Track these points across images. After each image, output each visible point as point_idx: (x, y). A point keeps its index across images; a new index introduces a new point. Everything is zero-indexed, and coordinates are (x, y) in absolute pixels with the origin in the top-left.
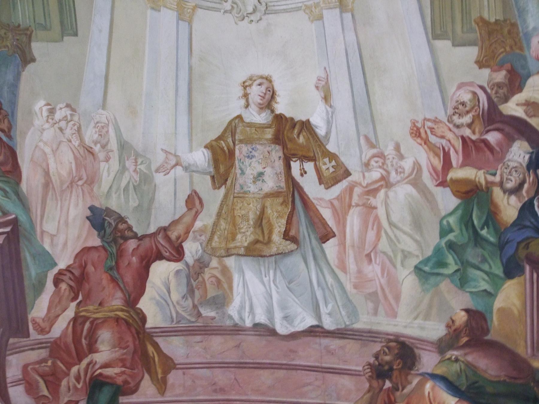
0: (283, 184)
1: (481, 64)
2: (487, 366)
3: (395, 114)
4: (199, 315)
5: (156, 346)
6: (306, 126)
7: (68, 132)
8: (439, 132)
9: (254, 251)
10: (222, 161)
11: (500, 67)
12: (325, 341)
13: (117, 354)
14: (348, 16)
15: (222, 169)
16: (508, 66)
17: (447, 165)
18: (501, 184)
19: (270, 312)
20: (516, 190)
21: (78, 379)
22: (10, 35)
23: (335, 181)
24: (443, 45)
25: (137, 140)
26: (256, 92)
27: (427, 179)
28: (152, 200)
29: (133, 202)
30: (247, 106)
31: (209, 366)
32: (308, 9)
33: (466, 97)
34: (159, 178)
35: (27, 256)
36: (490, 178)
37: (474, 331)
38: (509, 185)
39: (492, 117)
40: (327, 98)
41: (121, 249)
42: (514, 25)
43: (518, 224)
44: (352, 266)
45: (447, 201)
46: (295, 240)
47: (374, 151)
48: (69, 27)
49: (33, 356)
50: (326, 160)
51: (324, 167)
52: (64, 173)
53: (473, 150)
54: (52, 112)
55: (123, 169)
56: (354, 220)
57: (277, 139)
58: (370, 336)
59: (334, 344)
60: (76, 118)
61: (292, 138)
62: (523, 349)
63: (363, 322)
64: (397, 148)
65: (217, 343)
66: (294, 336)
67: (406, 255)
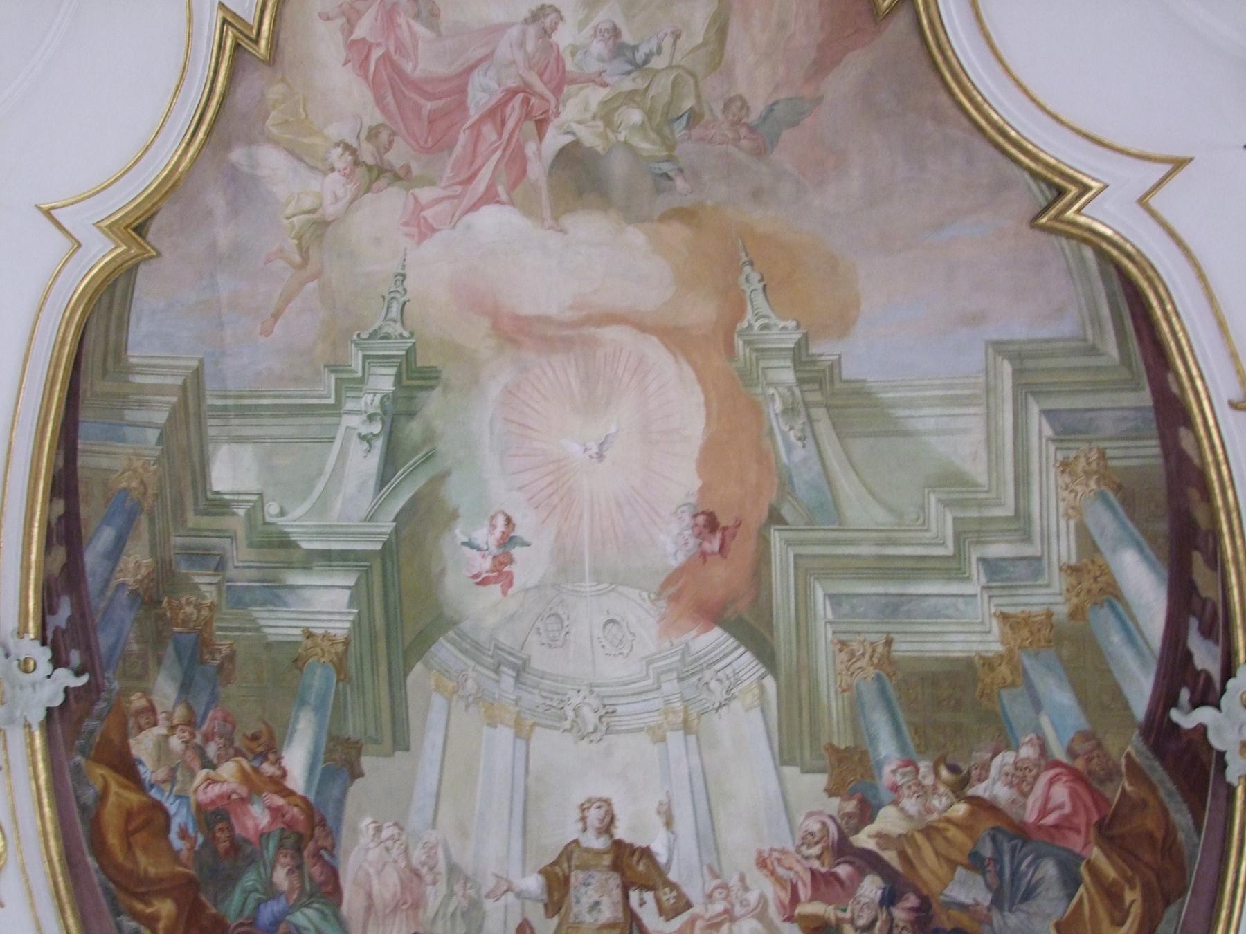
0: (620, 915)
1: (831, 792)
3: (740, 844)
6: (646, 853)
7: (395, 852)
8: (787, 862)
10: (557, 886)
11: (850, 797)
14: (692, 739)
15: (556, 896)
16: (858, 795)
17: (795, 899)
18: (852, 921)
22: (339, 748)
23: (676, 912)
24: (791, 772)
25: (467, 862)
26: (594, 815)
27: (773, 913)
28: (481, 927)
30: (585, 830)
32: (651, 730)
33: (815, 826)
34: (489, 905)
36: (841, 914)
38: (861, 922)
39: (842, 849)
40: (669, 824)
42: (864, 753)
47: (717, 882)
48: (400, 739)
50: (667, 890)
51: (664, 898)
52: (388, 896)
53: (823, 883)
54: (378, 830)
55: (451, 894)
57: (616, 866)
60: (404, 837)
61: (631, 865)
64: (742, 879)
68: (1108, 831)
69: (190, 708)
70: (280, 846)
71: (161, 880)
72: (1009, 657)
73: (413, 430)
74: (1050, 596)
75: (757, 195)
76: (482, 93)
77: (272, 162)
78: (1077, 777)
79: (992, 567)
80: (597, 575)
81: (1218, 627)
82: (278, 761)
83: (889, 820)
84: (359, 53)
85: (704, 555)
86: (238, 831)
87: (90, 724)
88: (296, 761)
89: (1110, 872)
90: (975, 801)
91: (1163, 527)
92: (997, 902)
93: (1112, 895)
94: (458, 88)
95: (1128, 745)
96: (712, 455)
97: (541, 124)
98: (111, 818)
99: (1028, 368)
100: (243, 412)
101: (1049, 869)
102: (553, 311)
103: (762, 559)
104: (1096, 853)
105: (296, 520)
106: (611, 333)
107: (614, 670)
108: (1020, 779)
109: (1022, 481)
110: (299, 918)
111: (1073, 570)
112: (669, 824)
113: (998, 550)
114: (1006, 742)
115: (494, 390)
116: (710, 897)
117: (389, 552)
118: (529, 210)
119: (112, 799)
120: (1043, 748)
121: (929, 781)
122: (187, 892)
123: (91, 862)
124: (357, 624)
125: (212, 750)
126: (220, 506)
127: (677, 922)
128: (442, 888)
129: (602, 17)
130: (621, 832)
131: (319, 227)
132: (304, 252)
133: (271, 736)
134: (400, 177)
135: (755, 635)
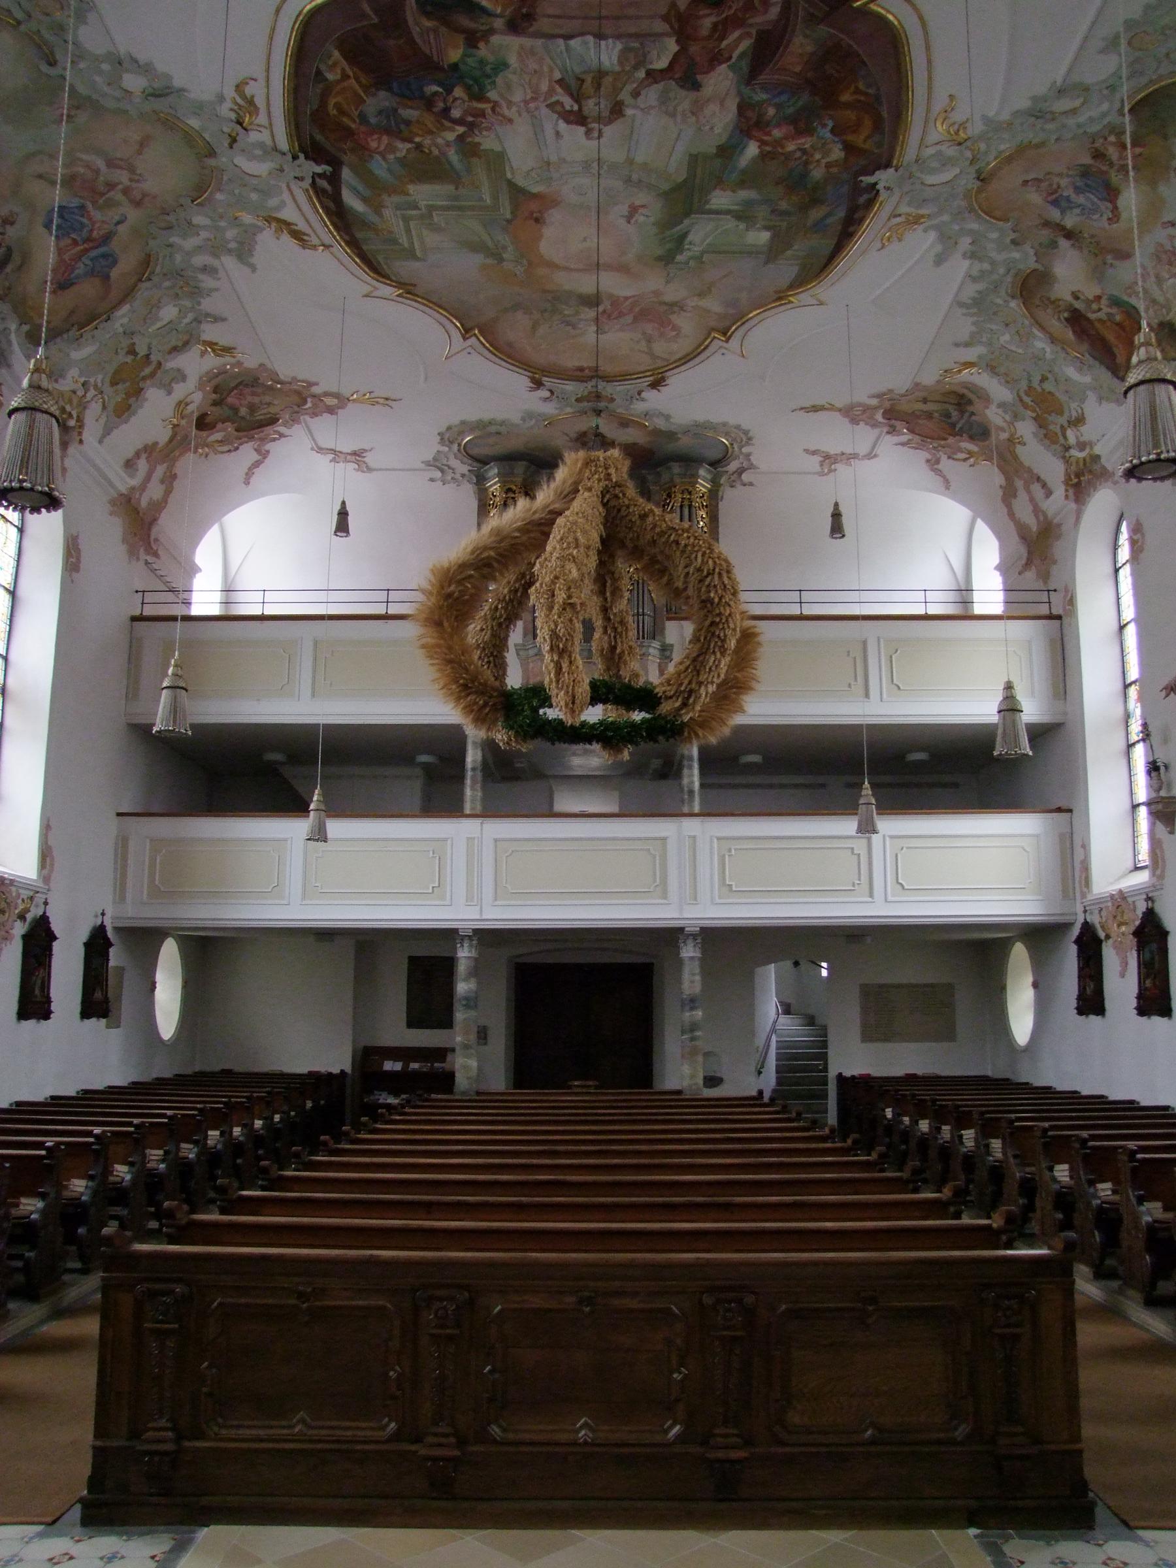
2: (465, 22)
3: (522, 126)
4: (642, 44)
5: (672, 27)
6: (568, 122)
10: (617, 111)
11: (469, 143)
12: (562, 32)
20: (455, 99)
21: (730, 7)
24: (498, 148)
27: (504, 104)
29: (672, 95)
31: (638, 17)
33: (485, 133)
34: (655, 103)
35: (746, 70)
37: (472, 40)
40: (557, 133)
41: (686, 74)
43: (454, 87)
44: (546, 69)
45: (492, 95)
46: (578, 79)
48: (694, 160)
49: (758, 19)
54: (712, 128)
56: (544, 87)
59: (557, 31)
61: (578, 118)
63: (539, 42)
65: (633, 30)
66: (582, 34)
67: (515, 73)
68: (349, 133)
73: (668, 246)
74: (390, 201)
76: (629, 319)
79: (416, 208)
81: (319, 192)
83: (451, 136)
85: (540, 212)
86: (791, 128)
89: (345, 119)
90: (410, 141)
92: (396, 110)
93: (342, 112)
94: (636, 319)
97: (604, 311)
98: (865, 131)
100: (750, 253)
101: (373, 120)
104: (353, 126)
105: (730, 223)
109: (408, 231)
110: (765, 96)
111: (383, 207)
112: (557, 133)
113: (414, 212)
114: (402, 161)
116: (537, 109)
117: (687, 214)
118: (611, 296)
119: (862, 137)
120: (384, 158)
121: (433, 149)
123: (885, 114)
125: (798, 154)
126: (767, 228)
127: (554, 99)
128: (680, 109)
130: (582, 129)
131: (701, 295)
132: (709, 289)
135: (518, 194)
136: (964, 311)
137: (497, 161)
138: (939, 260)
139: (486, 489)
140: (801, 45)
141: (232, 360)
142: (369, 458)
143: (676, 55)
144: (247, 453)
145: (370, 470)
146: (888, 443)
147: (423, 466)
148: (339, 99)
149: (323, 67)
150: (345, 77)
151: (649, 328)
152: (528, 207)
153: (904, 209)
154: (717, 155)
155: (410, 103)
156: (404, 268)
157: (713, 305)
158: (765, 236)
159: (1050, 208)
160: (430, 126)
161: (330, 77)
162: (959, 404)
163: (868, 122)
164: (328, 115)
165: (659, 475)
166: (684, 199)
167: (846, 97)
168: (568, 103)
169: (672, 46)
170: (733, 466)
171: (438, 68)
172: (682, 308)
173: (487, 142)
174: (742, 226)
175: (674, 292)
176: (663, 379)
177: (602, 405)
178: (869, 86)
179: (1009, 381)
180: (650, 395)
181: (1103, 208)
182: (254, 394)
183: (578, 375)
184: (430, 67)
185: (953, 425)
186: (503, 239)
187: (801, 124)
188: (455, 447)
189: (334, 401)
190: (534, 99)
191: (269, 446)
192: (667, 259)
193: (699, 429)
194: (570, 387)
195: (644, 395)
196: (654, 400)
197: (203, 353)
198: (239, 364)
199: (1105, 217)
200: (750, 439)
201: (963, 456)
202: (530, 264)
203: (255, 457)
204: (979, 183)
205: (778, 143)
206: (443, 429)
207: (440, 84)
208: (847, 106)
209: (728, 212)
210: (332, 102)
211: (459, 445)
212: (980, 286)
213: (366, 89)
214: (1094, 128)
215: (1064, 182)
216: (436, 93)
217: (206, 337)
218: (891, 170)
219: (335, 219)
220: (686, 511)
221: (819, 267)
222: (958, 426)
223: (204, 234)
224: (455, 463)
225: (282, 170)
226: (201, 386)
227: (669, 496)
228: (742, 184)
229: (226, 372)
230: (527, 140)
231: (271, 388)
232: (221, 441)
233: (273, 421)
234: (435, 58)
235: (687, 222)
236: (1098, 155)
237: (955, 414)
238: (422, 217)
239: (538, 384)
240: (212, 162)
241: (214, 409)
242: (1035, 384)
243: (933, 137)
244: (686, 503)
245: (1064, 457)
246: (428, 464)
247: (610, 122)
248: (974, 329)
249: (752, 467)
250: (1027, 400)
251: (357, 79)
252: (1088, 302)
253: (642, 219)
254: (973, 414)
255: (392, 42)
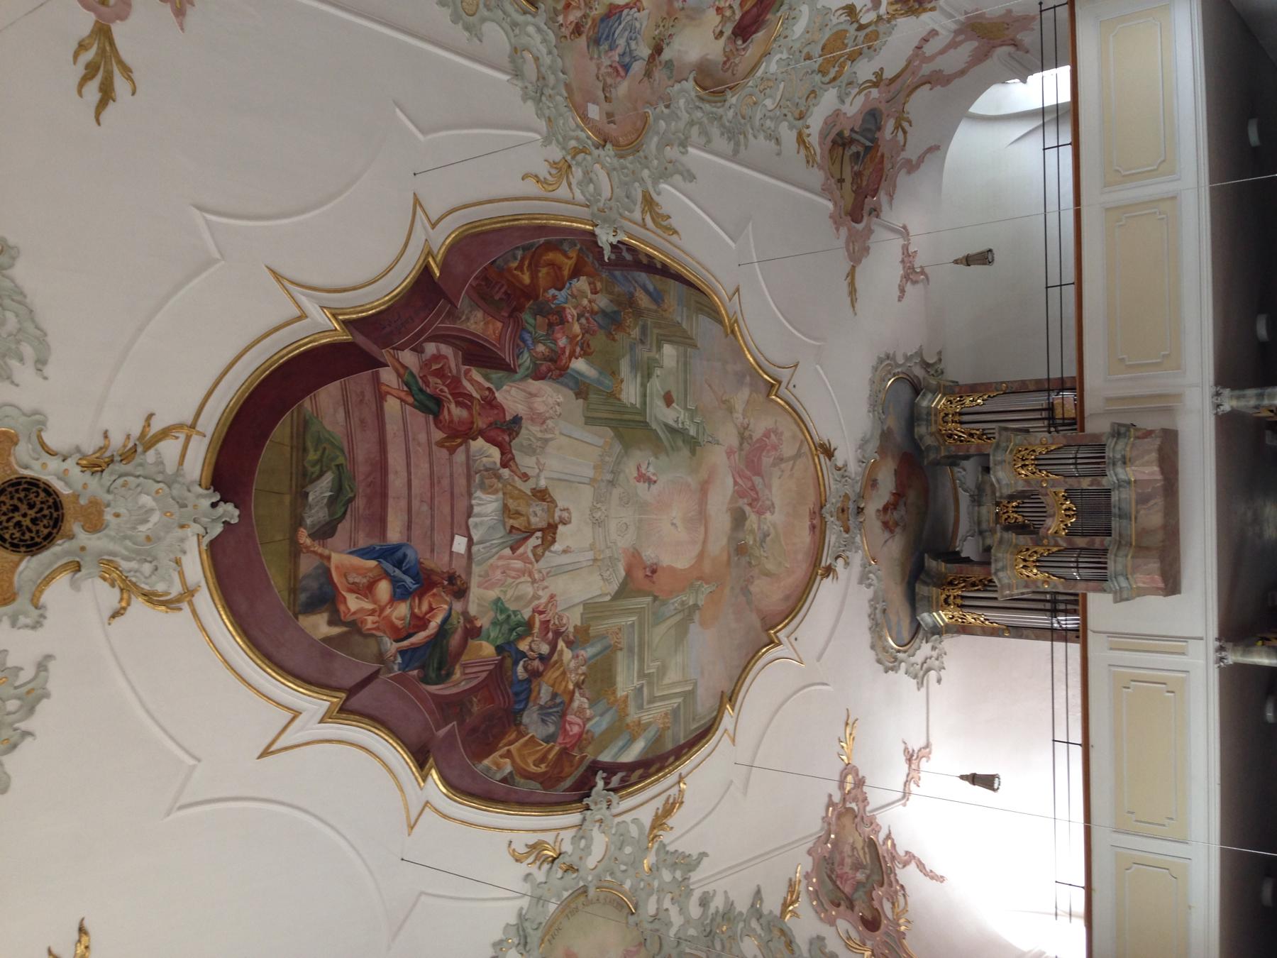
1: (575, 627)
3: (558, 585)
5: (460, 445)
6: (554, 541)
9: (505, 508)
10: (542, 495)
13: (456, 419)
19: (479, 515)
20: (531, 649)
21: (442, 391)
23: (534, 555)
24: (580, 609)
26: (565, 515)
27: (536, 602)
29: (525, 443)
31: (452, 475)
34: (534, 459)
35: (501, 374)
37: (473, 632)
40: (565, 552)
41: (504, 431)
44: (500, 563)
45: (527, 614)
46: (511, 532)
48: (590, 421)
49: (453, 365)
54: (558, 404)
56: (518, 564)
58: (469, 573)
61: (550, 532)
62: (465, 658)
63: (476, 569)
67: (505, 592)
68: (565, 753)
69: (596, 313)
70: (552, 350)
71: (537, 277)
72: (616, 701)
73: (680, 443)
74: (633, 715)
75: (732, 588)
76: (757, 480)
77: (745, 393)
78: (580, 735)
79: (640, 689)
80: (641, 521)
81: (624, 785)
82: (580, 356)
83: (568, 654)
84: (767, 434)
87: (591, 256)
88: (579, 365)
89: (551, 756)
90: (573, 692)
91: (650, 756)
92: (542, 708)
93: (543, 759)
94: (758, 474)
95: (590, 754)
96: (672, 570)
97: (750, 505)
99: (689, 696)
100: (685, 364)
101: (552, 729)
102: (709, 507)
103: (646, 594)
104: (557, 748)
106: (702, 529)
107: (613, 525)
108: (581, 710)
109: (663, 698)
112: (565, 552)
113: (645, 690)
114: (593, 702)
115: (690, 480)
116: (540, 572)
117: (645, 425)
120: (589, 719)
122: (530, 293)
123: (542, 240)
124: (625, 406)
125: (583, 321)
126: (659, 348)
127: (530, 555)
128: (539, 435)
129: (772, 530)
130: (561, 528)
131: (731, 410)
132: (724, 402)
133: (589, 354)
134: (741, 448)
135: (625, 591)
136: (742, 147)
137: (592, 609)
138: (690, 176)
139: (946, 625)
140: (477, 323)
141: (804, 882)
142: (915, 745)
143: (489, 440)
144: (908, 876)
145: (928, 746)
146: (888, 215)
147: (923, 690)
148: (530, 760)
149: (499, 776)
150: (508, 755)
151: (767, 460)
152: (640, 579)
153: (637, 215)
154: (585, 399)
155: (534, 694)
156: (704, 704)
157: (741, 398)
158: (669, 350)
159: (631, 72)
160: (558, 673)
161: (508, 768)
162: (844, 145)
163: (550, 256)
164: (545, 773)
165: (929, 448)
166: (630, 428)
167: (526, 279)
168: (534, 541)
169: (479, 444)
170: (918, 372)
171: (500, 666)
172: (746, 428)
173: (573, 619)
174: (658, 371)
175: (728, 435)
176: (822, 446)
177: (851, 506)
178: (515, 258)
179: (813, 94)
180: (840, 458)
181: (629, 18)
182: (842, 863)
183: (819, 531)
184: (498, 674)
185: (867, 149)
186: (675, 603)
187: (557, 318)
188: (900, 655)
189: (850, 778)
190: (530, 575)
191: (901, 852)
192: (693, 444)
193: (879, 404)
194: (832, 538)
195: (840, 464)
196: (847, 454)
197: (794, 913)
198: (807, 876)
199: (637, 15)
200: (888, 357)
201: (900, 133)
202: (699, 578)
203: (912, 866)
204: (609, 146)
205: (572, 339)
206: (881, 668)
207: (516, 663)
208: (534, 276)
209: (643, 385)
210: (533, 769)
211: (899, 651)
212: (715, 131)
213: (521, 735)
214: (551, 36)
215: (606, 62)
216: (525, 668)
217: (777, 912)
218: (597, 231)
219: (653, 769)
220: (965, 418)
221: (697, 295)
222: (868, 144)
223: (667, 904)
224: (919, 657)
225: (601, 821)
226: (832, 923)
227: (950, 436)
228: (614, 373)
229: (816, 892)
230: (571, 581)
231: (835, 844)
232: (893, 904)
233: (872, 844)
234: (491, 667)
235: (654, 426)
236: (577, 30)
237: (854, 149)
238: (650, 684)
239: (829, 570)
240: (592, 892)
241: (857, 909)
242: (816, 66)
243: (563, 191)
244: (957, 418)
245: (889, 21)
246: (920, 685)
247: (553, 501)
248: (761, 136)
249: (919, 353)
250: (832, 75)
251: (511, 743)
252: (724, 20)
253: (651, 469)
254: (852, 130)
255: (475, 709)
